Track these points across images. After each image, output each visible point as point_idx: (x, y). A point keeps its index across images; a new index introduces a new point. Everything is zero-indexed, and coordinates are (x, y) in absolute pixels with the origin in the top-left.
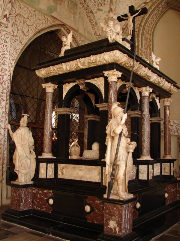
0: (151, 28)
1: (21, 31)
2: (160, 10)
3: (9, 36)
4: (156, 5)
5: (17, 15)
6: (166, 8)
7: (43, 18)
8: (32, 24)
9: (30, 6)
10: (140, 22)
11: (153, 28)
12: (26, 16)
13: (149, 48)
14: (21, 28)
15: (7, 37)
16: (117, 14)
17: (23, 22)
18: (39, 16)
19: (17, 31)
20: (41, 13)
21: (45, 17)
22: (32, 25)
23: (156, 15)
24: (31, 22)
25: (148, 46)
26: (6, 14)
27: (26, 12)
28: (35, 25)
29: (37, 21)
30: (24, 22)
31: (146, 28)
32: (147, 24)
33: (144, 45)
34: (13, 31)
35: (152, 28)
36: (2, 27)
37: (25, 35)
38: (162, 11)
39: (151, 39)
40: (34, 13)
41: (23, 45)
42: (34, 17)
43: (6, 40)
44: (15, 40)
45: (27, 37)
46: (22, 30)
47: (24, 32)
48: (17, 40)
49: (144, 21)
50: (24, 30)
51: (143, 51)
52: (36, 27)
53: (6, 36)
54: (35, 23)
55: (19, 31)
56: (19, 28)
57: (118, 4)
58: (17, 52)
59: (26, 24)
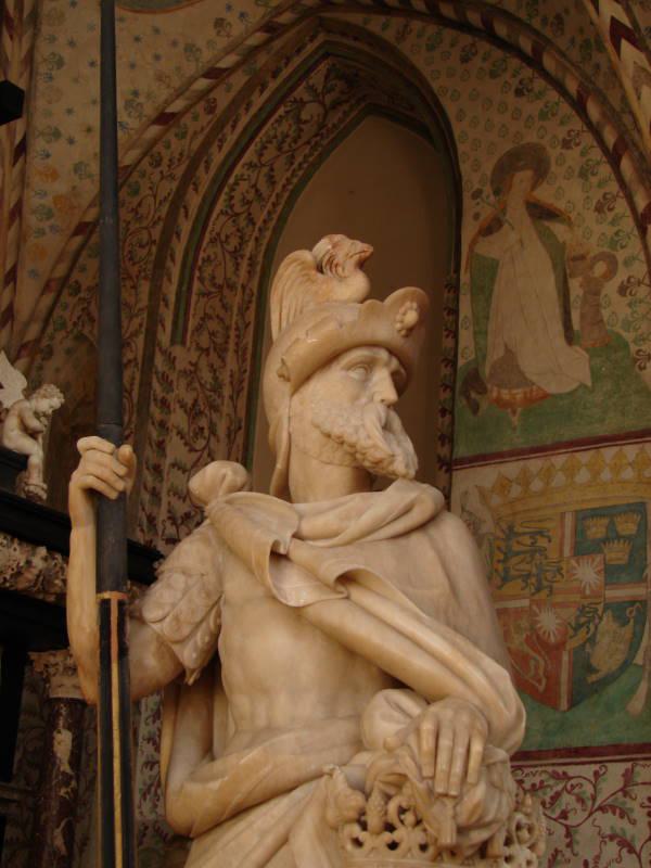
0: (259, 223)
2: (304, 116)
4: (273, 85)
6: (346, 107)
10: (174, 185)
11: (272, 224)
13: (237, 344)
16: (42, 134)
23: (286, 147)
25: (232, 333)
31: (217, 223)
32: (223, 197)
33: (192, 324)
35: (265, 222)
38: (322, 126)
39: (255, 291)
49: (205, 178)
51: (181, 365)
57: (51, 78)
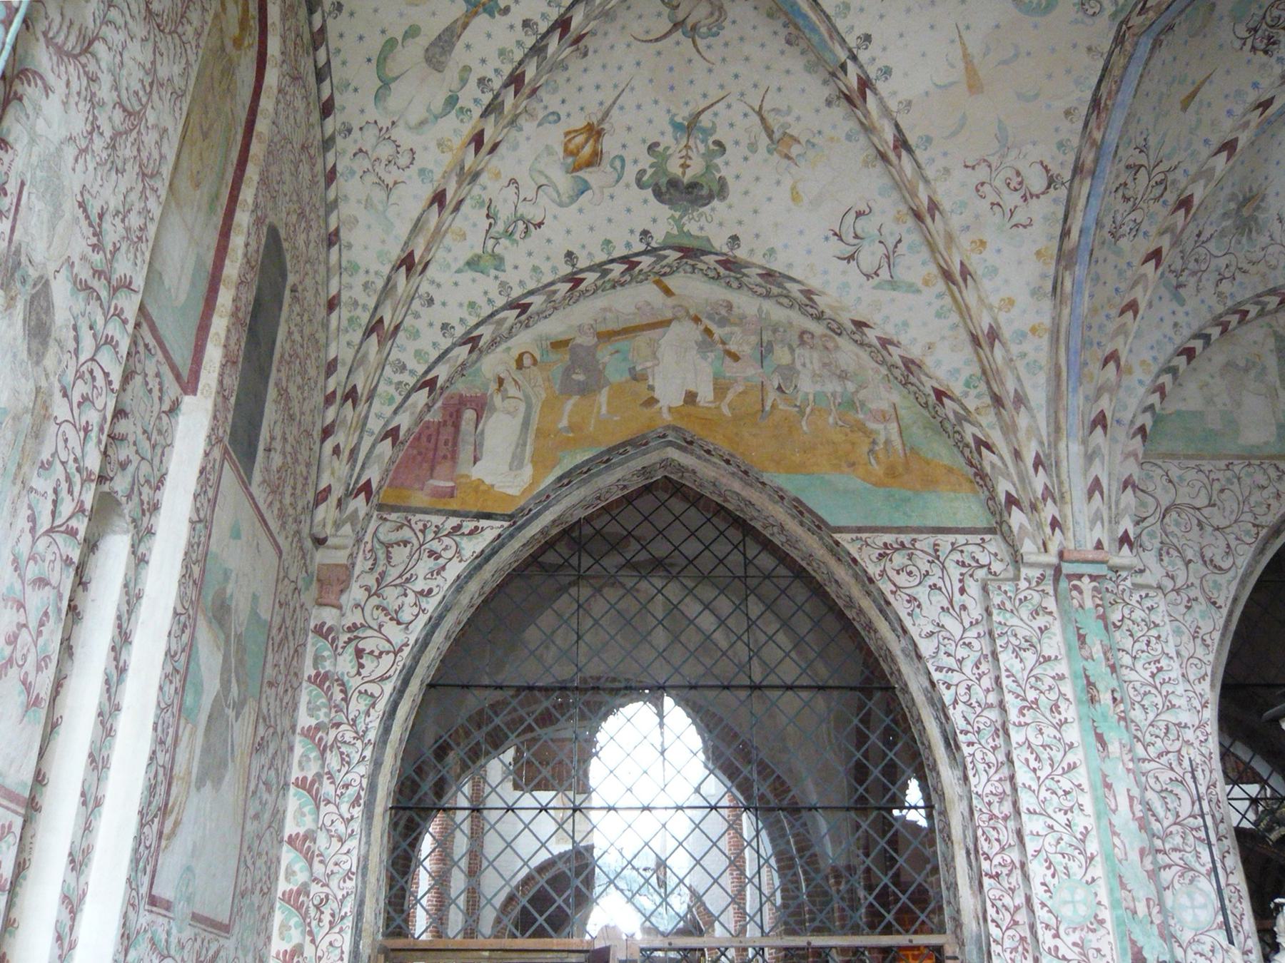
1: (1200, 562)
3: (1156, 599)
5: (1167, 510)
7: (1273, 473)
8: (1233, 517)
9: (1202, 458)
12: (1201, 501)
14: (1197, 549)
15: (1151, 609)
17: (1196, 528)
18: (1249, 475)
19: (1183, 567)
20: (1258, 462)
21: (1278, 468)
22: (1236, 521)
24: (1227, 513)
26: (1126, 532)
27: (1199, 484)
28: (1248, 517)
29: (1253, 500)
30: (1200, 524)
34: (1168, 575)
36: (1125, 579)
37: (1220, 569)
40: (1229, 474)
41: (1225, 611)
42: (1236, 487)
43: (1153, 618)
44: (1185, 602)
45: (1232, 573)
46: (1203, 557)
47: (1212, 561)
48: (1196, 599)
50: (1208, 554)
52: (1257, 522)
53: (1148, 603)
54: (1246, 509)
55: (1191, 565)
56: (1190, 554)
58: (1209, 642)
59: (1209, 529)
